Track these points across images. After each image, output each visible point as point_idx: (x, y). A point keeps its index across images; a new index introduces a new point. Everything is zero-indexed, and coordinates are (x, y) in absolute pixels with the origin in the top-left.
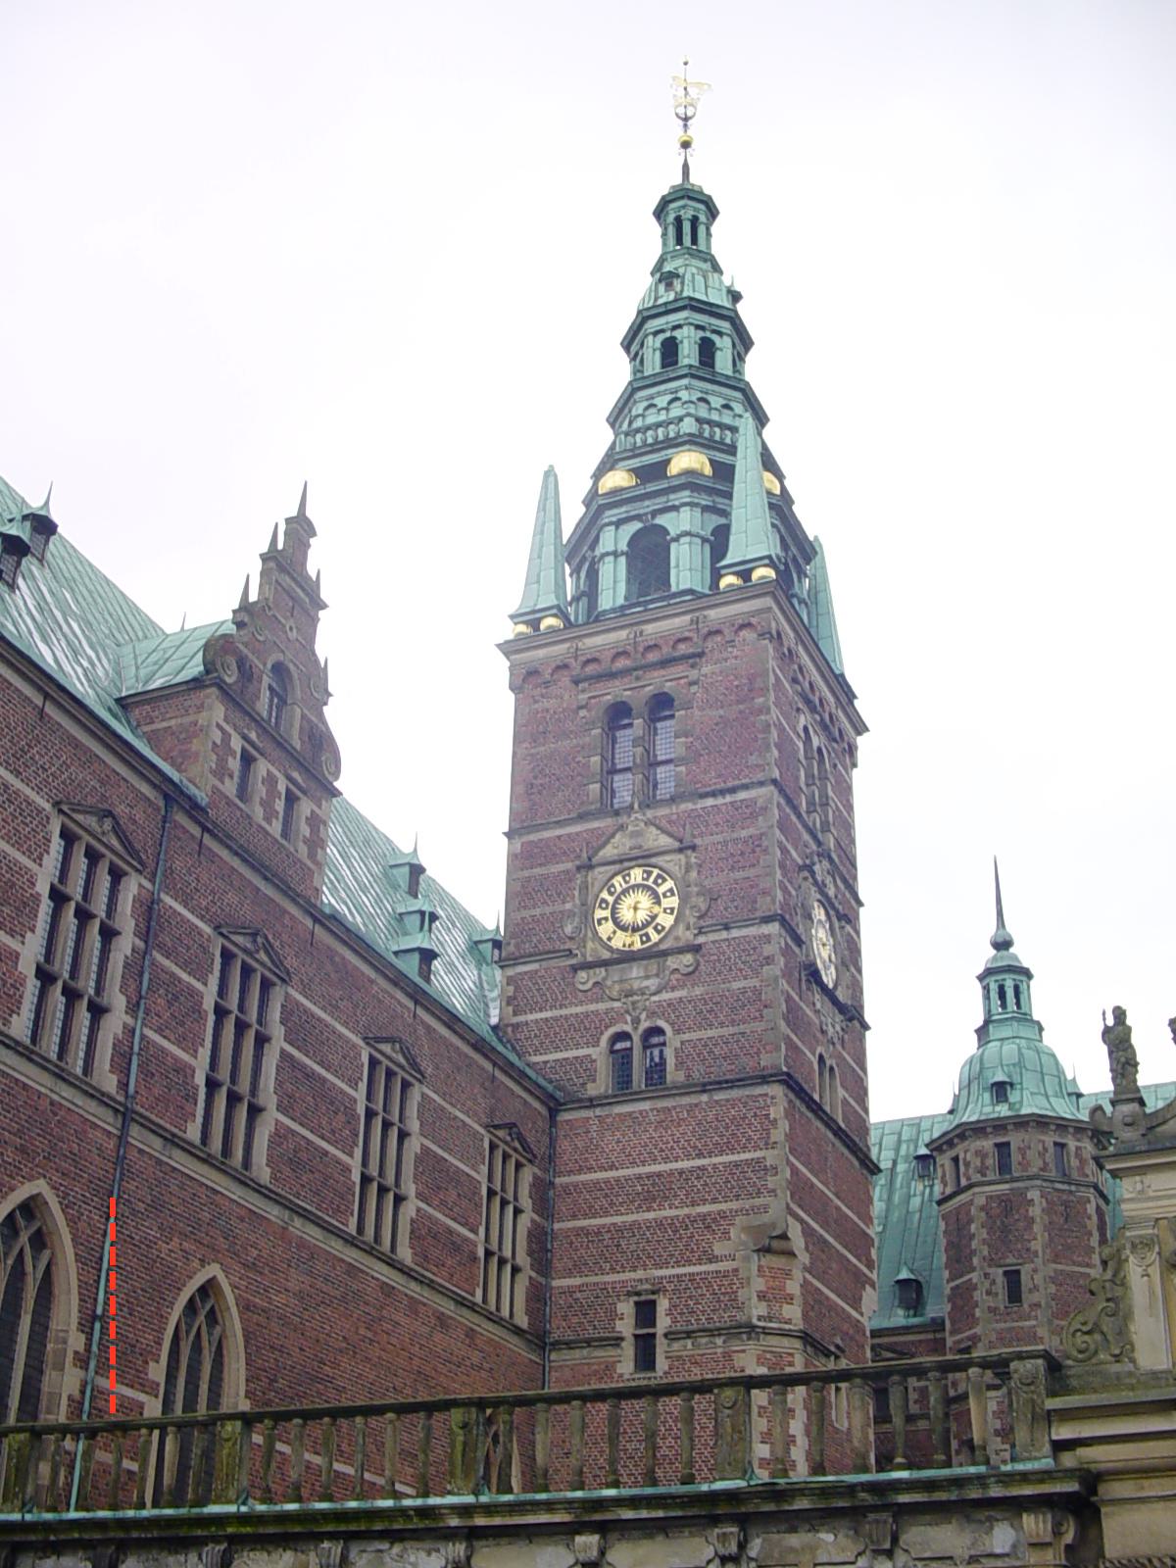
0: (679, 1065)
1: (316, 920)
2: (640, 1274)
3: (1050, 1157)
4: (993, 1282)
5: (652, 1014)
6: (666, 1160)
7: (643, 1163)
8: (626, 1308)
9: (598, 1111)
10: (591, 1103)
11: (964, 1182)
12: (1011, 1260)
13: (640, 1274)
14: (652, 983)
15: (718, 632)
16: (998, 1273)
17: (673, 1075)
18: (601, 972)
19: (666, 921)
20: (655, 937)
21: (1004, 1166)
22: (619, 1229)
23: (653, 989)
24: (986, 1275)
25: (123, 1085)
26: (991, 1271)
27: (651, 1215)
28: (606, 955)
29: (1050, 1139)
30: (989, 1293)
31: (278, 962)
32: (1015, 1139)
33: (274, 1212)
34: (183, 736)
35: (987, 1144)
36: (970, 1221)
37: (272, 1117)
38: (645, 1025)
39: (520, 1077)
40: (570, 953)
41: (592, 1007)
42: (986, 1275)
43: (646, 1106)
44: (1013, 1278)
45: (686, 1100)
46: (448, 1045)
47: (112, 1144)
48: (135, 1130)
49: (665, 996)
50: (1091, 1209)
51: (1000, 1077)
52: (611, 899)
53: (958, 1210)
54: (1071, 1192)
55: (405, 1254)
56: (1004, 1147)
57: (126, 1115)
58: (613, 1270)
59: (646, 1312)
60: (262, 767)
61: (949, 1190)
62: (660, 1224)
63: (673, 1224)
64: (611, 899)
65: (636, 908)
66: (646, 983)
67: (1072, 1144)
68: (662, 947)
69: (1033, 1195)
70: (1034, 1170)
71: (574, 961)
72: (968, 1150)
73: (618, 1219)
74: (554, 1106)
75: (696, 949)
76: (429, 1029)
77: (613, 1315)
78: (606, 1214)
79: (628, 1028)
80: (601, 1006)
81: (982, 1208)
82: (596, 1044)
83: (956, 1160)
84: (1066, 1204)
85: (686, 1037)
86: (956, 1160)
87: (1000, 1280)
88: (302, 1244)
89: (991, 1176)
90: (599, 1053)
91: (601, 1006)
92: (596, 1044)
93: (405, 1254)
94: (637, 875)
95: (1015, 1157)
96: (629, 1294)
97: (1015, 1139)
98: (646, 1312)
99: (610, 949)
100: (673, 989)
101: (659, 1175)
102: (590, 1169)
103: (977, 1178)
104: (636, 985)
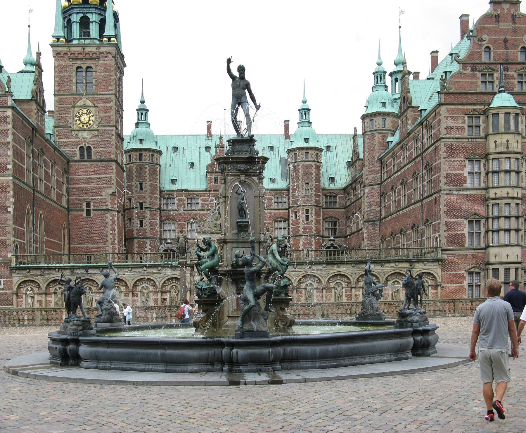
0: (94, 155)
1: (45, 141)
2: (87, 197)
3: (151, 158)
4: (137, 185)
5: (88, 143)
6: (92, 175)
7: (87, 175)
8: (84, 204)
9: (77, 163)
10: (76, 161)
11: (131, 162)
12: (141, 181)
13: (87, 197)
14: (89, 137)
15: (103, 53)
16: (138, 183)
17: (93, 157)
18: (77, 133)
19: (91, 122)
20: (89, 126)
21: (141, 159)
22: (83, 188)
23: (89, 138)
24: (136, 183)
25: (33, 184)
26: (137, 182)
27: (89, 186)
28: (78, 129)
29: (151, 154)
30: (136, 187)
31: (43, 152)
32: (144, 153)
33: (44, 199)
34: (29, 111)
35: (137, 154)
36: (133, 171)
37: (44, 181)
38: (87, 145)
39: (61, 154)
40: (70, 127)
41: (76, 140)
42: (136, 183)
43: (88, 163)
44: (141, 184)
45: (96, 163)
46: (58, 155)
47: (32, 195)
48: (35, 192)
49: (91, 140)
50: (158, 170)
51: (141, 138)
52: (79, 116)
53: (130, 167)
54: (154, 166)
55: (55, 200)
56: (141, 155)
57: (34, 190)
58: (82, 196)
59: (88, 205)
60: (40, 113)
61: (128, 163)
62: (91, 188)
63: (93, 188)
64: (79, 116)
65: (85, 118)
66: (87, 136)
67: (155, 155)
68: (91, 129)
69: (147, 166)
70: (147, 161)
71: (71, 129)
72: (133, 154)
73: (82, 186)
74: (69, 161)
75: (98, 130)
76: (56, 154)
77: (82, 205)
78: (80, 185)
79: (83, 146)
80: (78, 140)
81: (136, 168)
82: (77, 148)
83: (130, 156)
84: (153, 169)
85: (96, 149)
86: (130, 156)
87: (139, 185)
88: (47, 203)
89: (138, 161)
90: (77, 150)
91: (78, 140)
92: (77, 148)
93: (55, 200)
94: (85, 111)
95: (143, 157)
96: (85, 201)
97: (144, 153)
98: (88, 205)
99: (79, 127)
100: (93, 138)
101: (91, 178)
102: (76, 175)
103: (135, 161)
104: (85, 136)
